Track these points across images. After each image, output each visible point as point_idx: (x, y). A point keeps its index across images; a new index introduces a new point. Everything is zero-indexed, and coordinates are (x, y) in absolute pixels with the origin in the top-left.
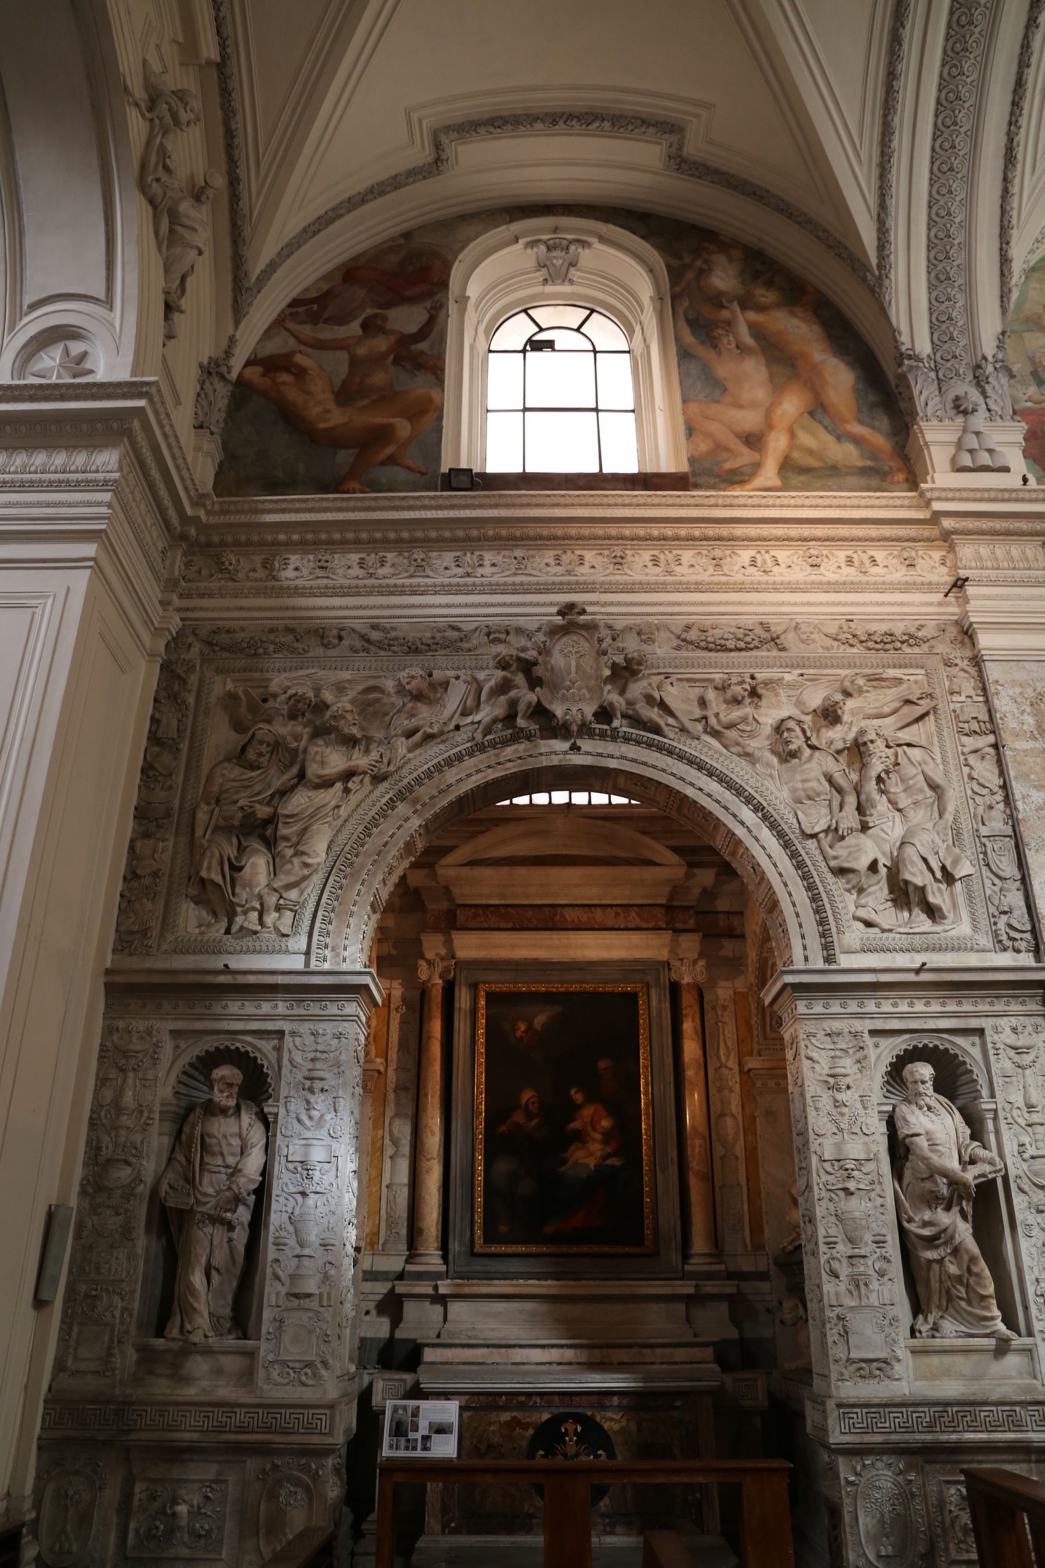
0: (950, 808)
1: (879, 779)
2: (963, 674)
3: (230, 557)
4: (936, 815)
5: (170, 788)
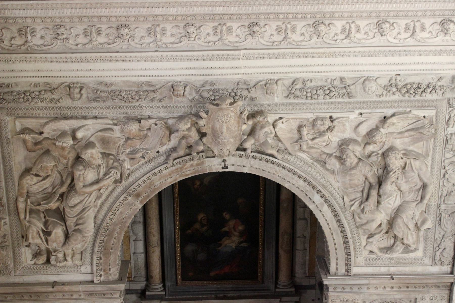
0: (427, 197)
4: (419, 198)
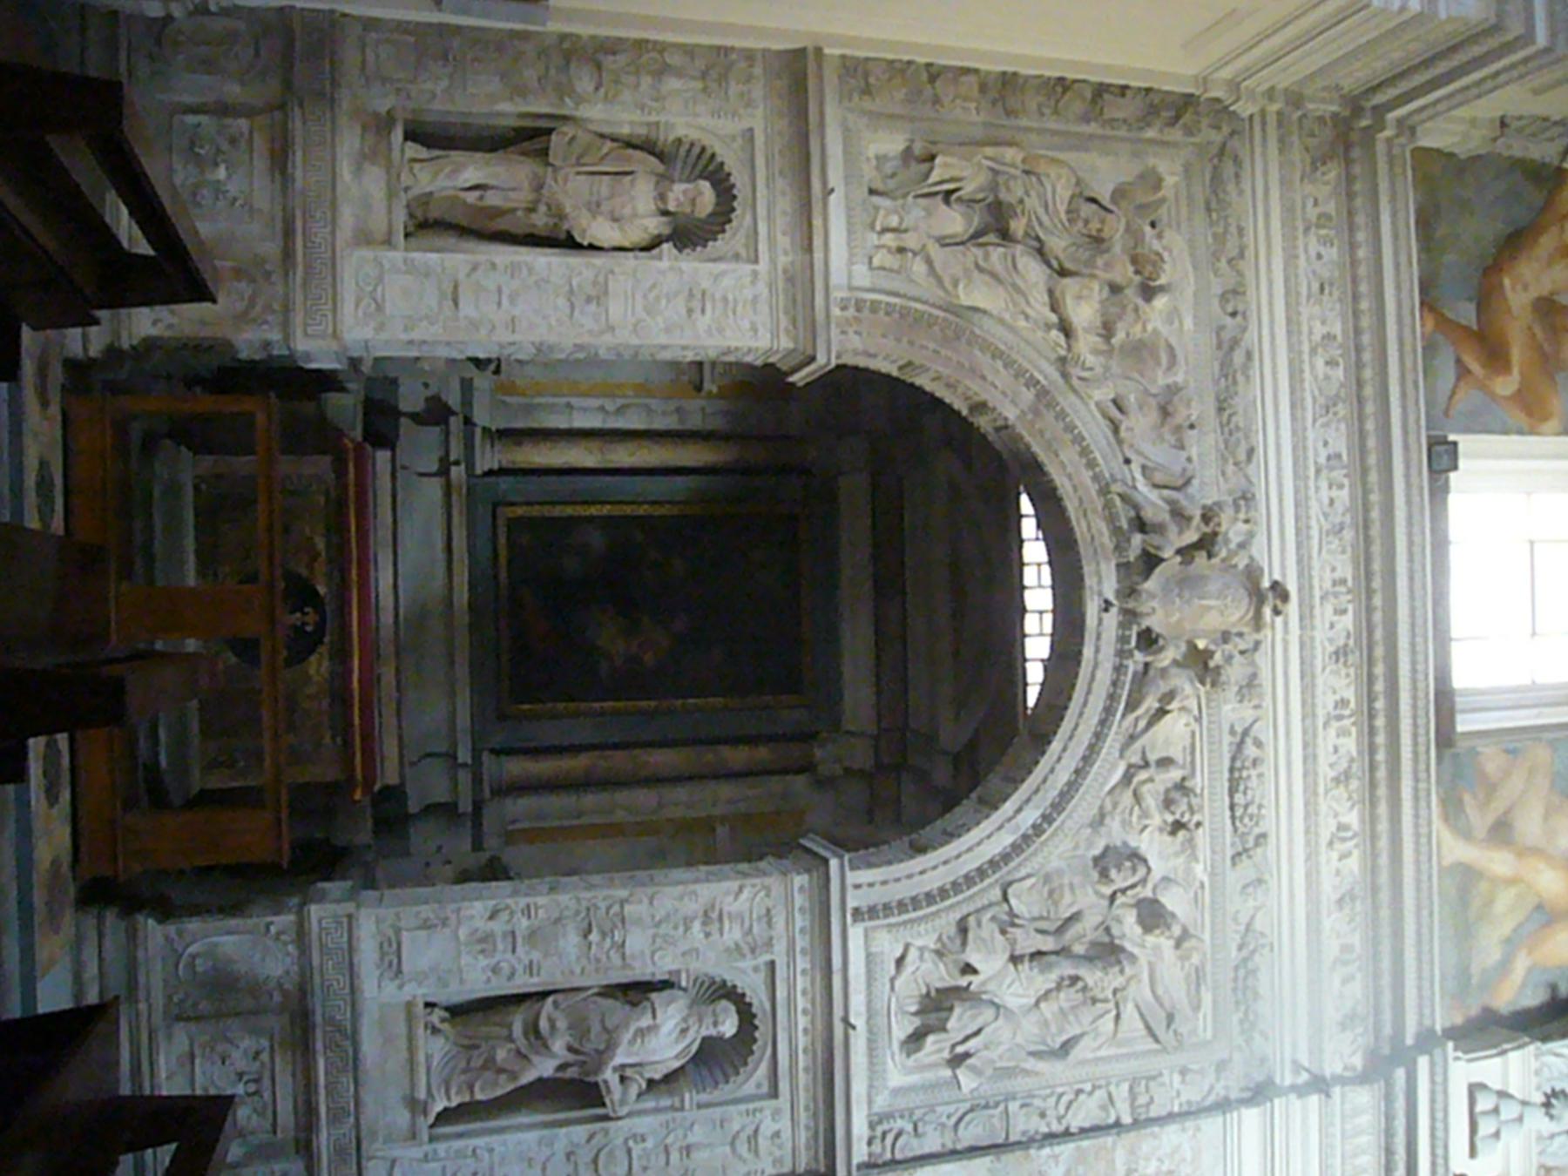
0: (1040, 1066)
1: (1075, 979)
2: (1206, 1088)
3: (1333, 172)
4: (1033, 1048)
5: (1042, 114)
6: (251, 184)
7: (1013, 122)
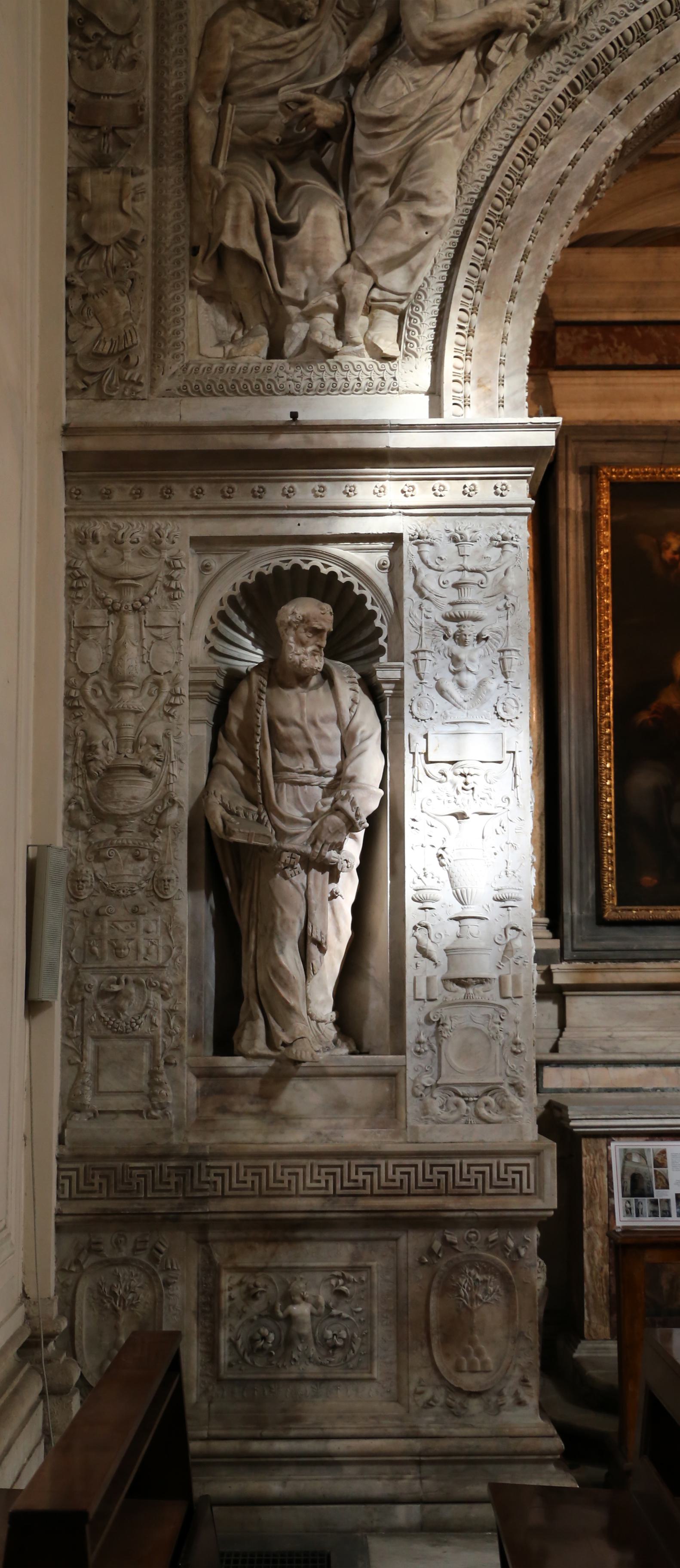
5: (133, 63)
6: (313, 1269)
7: (149, 110)
